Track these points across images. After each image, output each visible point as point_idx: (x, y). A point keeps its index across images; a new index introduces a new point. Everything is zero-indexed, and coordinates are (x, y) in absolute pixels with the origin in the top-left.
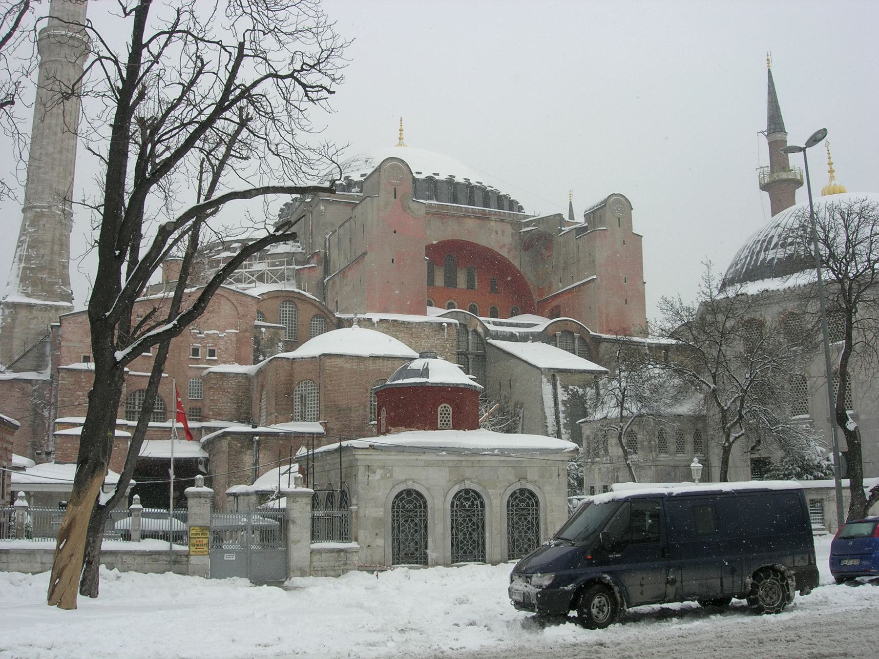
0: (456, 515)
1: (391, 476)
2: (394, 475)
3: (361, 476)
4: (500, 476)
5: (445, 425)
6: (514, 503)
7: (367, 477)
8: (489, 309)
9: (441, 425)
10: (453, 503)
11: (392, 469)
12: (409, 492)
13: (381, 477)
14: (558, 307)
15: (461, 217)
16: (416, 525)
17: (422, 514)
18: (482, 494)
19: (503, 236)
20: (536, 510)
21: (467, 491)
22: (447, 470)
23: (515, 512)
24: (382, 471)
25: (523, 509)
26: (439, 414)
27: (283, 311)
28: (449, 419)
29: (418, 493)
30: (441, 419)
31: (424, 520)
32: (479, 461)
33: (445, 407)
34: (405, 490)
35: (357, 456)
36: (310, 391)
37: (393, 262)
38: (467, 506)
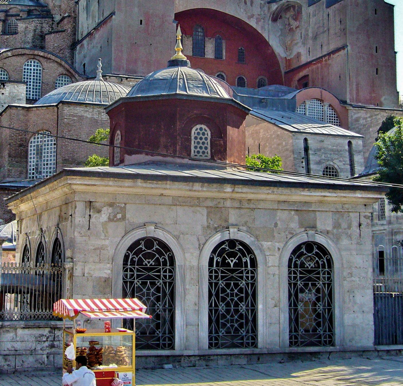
0: (216, 277)
1: (124, 218)
2: (128, 216)
3: (79, 219)
4: (279, 223)
5: (201, 154)
6: (299, 262)
7: (87, 217)
8: (236, 80)
9: (196, 154)
10: (211, 260)
11: (125, 207)
12: (149, 242)
13: (109, 218)
14: (306, 76)
16: (158, 290)
17: (168, 274)
18: (253, 248)
20: (329, 273)
21: (232, 243)
22: (205, 212)
23: (299, 275)
24: (110, 210)
25: (310, 272)
26: (193, 138)
27: (28, 69)
28: (206, 145)
30: (196, 145)
31: (170, 284)
32: (250, 200)
33: (201, 129)
34: (142, 239)
35: (74, 187)
36: (46, 143)
37: (141, 24)
38: (232, 264)
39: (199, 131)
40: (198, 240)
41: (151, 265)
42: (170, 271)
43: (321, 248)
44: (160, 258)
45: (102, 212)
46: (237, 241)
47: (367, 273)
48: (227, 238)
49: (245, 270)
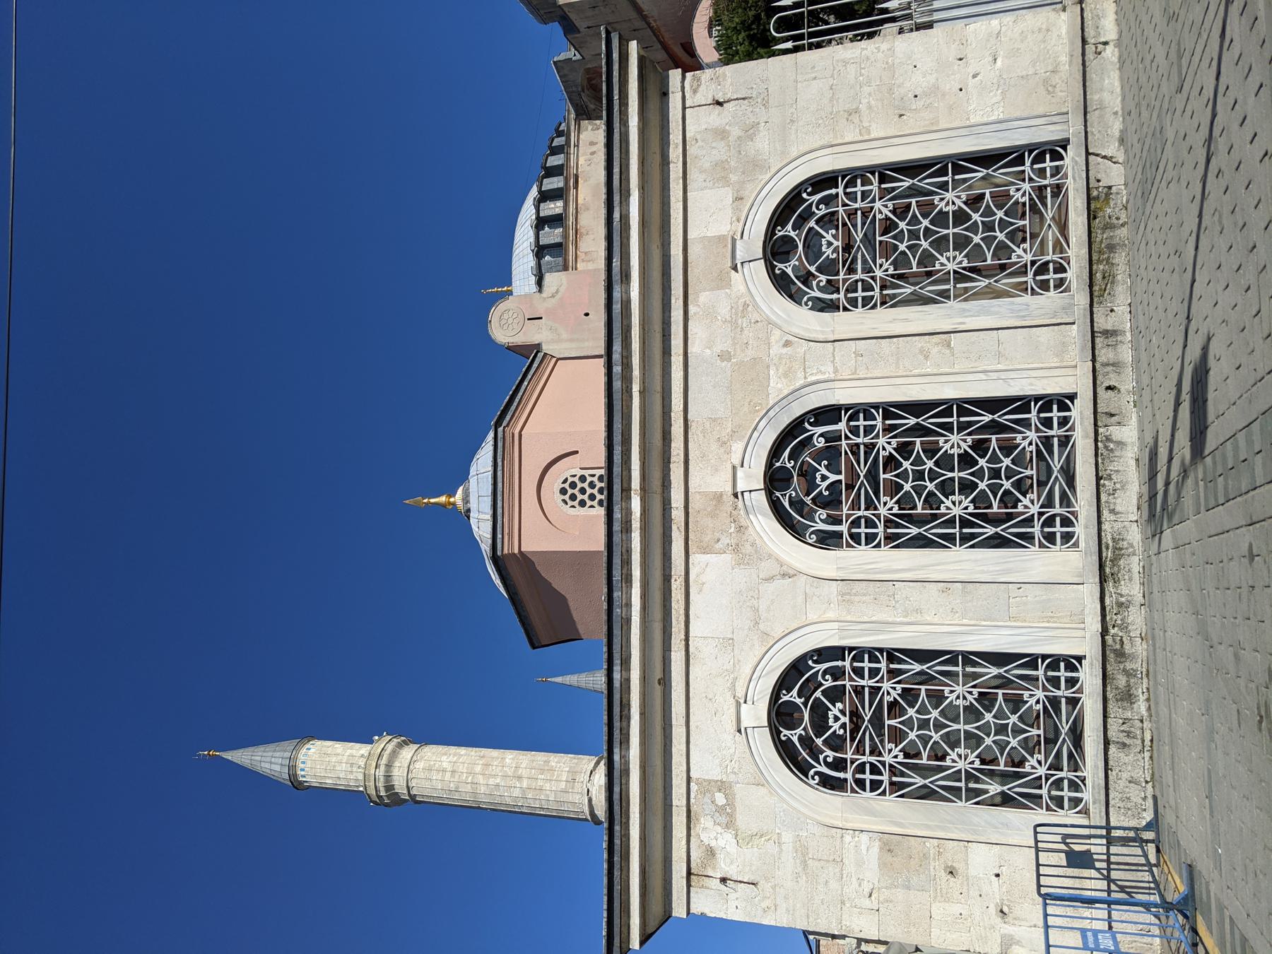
1: (723, 786)
4: (718, 348)
10: (828, 540)
12: (781, 715)
13: (728, 826)
15: (577, 208)
17: (866, 665)
18: (785, 420)
19: (597, 143)
21: (775, 480)
29: (784, 683)
38: (833, 478)
39: (567, 497)
40: (770, 579)
41: (843, 712)
42: (858, 658)
43: (781, 215)
44: (821, 685)
45: (713, 844)
46: (769, 464)
47: (845, 63)
48: (761, 497)
49: (847, 438)
